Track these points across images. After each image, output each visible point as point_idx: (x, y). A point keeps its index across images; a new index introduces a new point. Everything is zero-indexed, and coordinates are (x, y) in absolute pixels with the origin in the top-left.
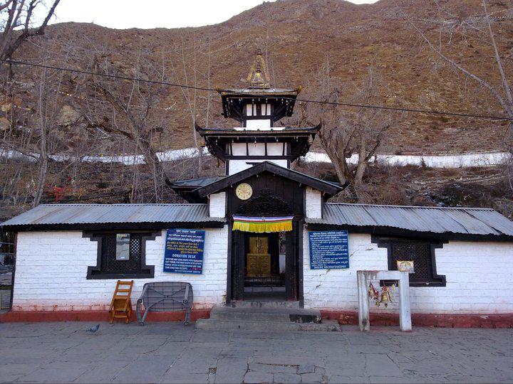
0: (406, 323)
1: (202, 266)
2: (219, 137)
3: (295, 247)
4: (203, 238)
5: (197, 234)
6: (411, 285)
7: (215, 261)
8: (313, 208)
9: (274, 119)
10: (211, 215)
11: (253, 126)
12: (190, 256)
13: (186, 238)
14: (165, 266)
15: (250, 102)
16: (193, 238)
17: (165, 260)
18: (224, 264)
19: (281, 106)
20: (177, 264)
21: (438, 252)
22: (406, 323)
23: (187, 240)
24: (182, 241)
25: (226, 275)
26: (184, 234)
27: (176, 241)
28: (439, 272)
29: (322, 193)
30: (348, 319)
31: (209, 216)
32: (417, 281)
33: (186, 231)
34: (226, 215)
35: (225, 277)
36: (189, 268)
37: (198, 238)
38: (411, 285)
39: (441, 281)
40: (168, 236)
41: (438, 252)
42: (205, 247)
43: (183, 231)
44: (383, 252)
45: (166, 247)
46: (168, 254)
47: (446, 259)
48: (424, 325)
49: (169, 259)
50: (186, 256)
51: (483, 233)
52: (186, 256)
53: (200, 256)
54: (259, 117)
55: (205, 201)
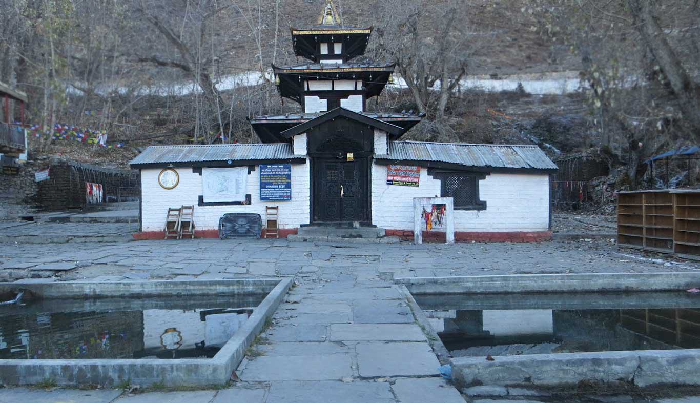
0: (450, 237)
4: (290, 171)
5: (284, 168)
6: (454, 209)
8: (380, 146)
9: (345, 57)
10: (296, 153)
11: (329, 64)
12: (280, 186)
13: (276, 172)
15: (323, 42)
16: (281, 172)
18: (307, 193)
19: (354, 45)
21: (481, 182)
22: (450, 237)
23: (277, 173)
25: (309, 202)
26: (274, 168)
27: (268, 175)
28: (481, 199)
29: (388, 132)
30: (406, 236)
31: (293, 154)
32: (465, 205)
36: (281, 196)
37: (285, 171)
38: (454, 209)
39: (482, 206)
40: (261, 171)
41: (481, 182)
44: (438, 183)
46: (263, 186)
47: (488, 188)
48: (465, 241)
51: (517, 166)
53: (288, 186)
54: (331, 55)
55: (289, 142)
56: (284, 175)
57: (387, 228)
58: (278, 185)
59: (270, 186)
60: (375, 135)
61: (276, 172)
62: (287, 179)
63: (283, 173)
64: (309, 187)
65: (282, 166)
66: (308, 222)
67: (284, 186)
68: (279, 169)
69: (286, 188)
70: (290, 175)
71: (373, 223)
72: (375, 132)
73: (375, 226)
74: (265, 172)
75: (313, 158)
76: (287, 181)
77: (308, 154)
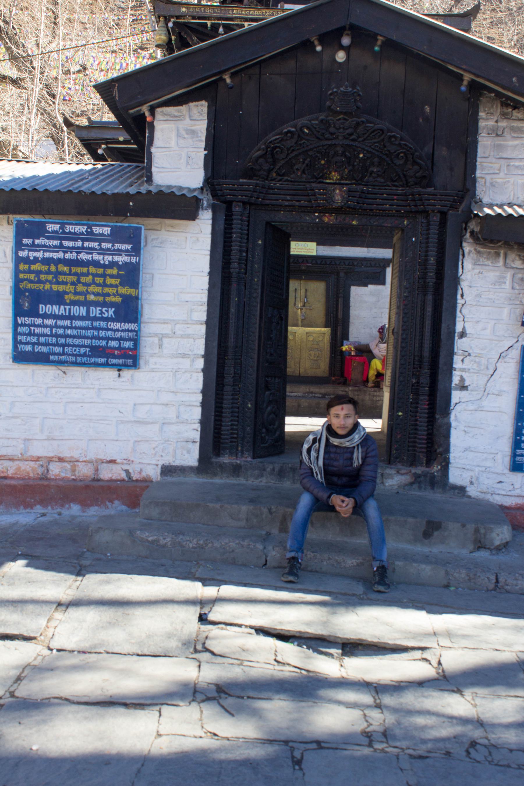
1: (136, 341)
2: (209, 23)
3: (430, 298)
4: (136, 250)
5: (117, 236)
7: (166, 329)
12: (95, 311)
13: (79, 250)
14: (16, 343)
16: (103, 252)
17: (16, 325)
20: (57, 336)
23: (84, 256)
24: (70, 263)
25: (200, 377)
27: (47, 261)
31: (150, 179)
33: (78, 229)
34: (208, 181)
35: (197, 381)
36: (96, 351)
37: (119, 252)
40: (19, 245)
42: (144, 277)
43: (69, 228)
45: (17, 281)
49: (28, 320)
50: (83, 311)
52: (83, 311)
53: (129, 310)
56: (112, 264)
57: (509, 502)
58: (87, 304)
59: (56, 309)
60: (482, 124)
61: (79, 250)
62: (122, 284)
63: (108, 258)
64: (204, 317)
65: (107, 230)
66: (191, 457)
67: (111, 312)
68: (97, 242)
69: (118, 318)
70: (138, 264)
71: (455, 477)
72: (482, 114)
73: (462, 489)
74: (34, 247)
75: (229, 204)
76: (125, 290)
77: (211, 182)
